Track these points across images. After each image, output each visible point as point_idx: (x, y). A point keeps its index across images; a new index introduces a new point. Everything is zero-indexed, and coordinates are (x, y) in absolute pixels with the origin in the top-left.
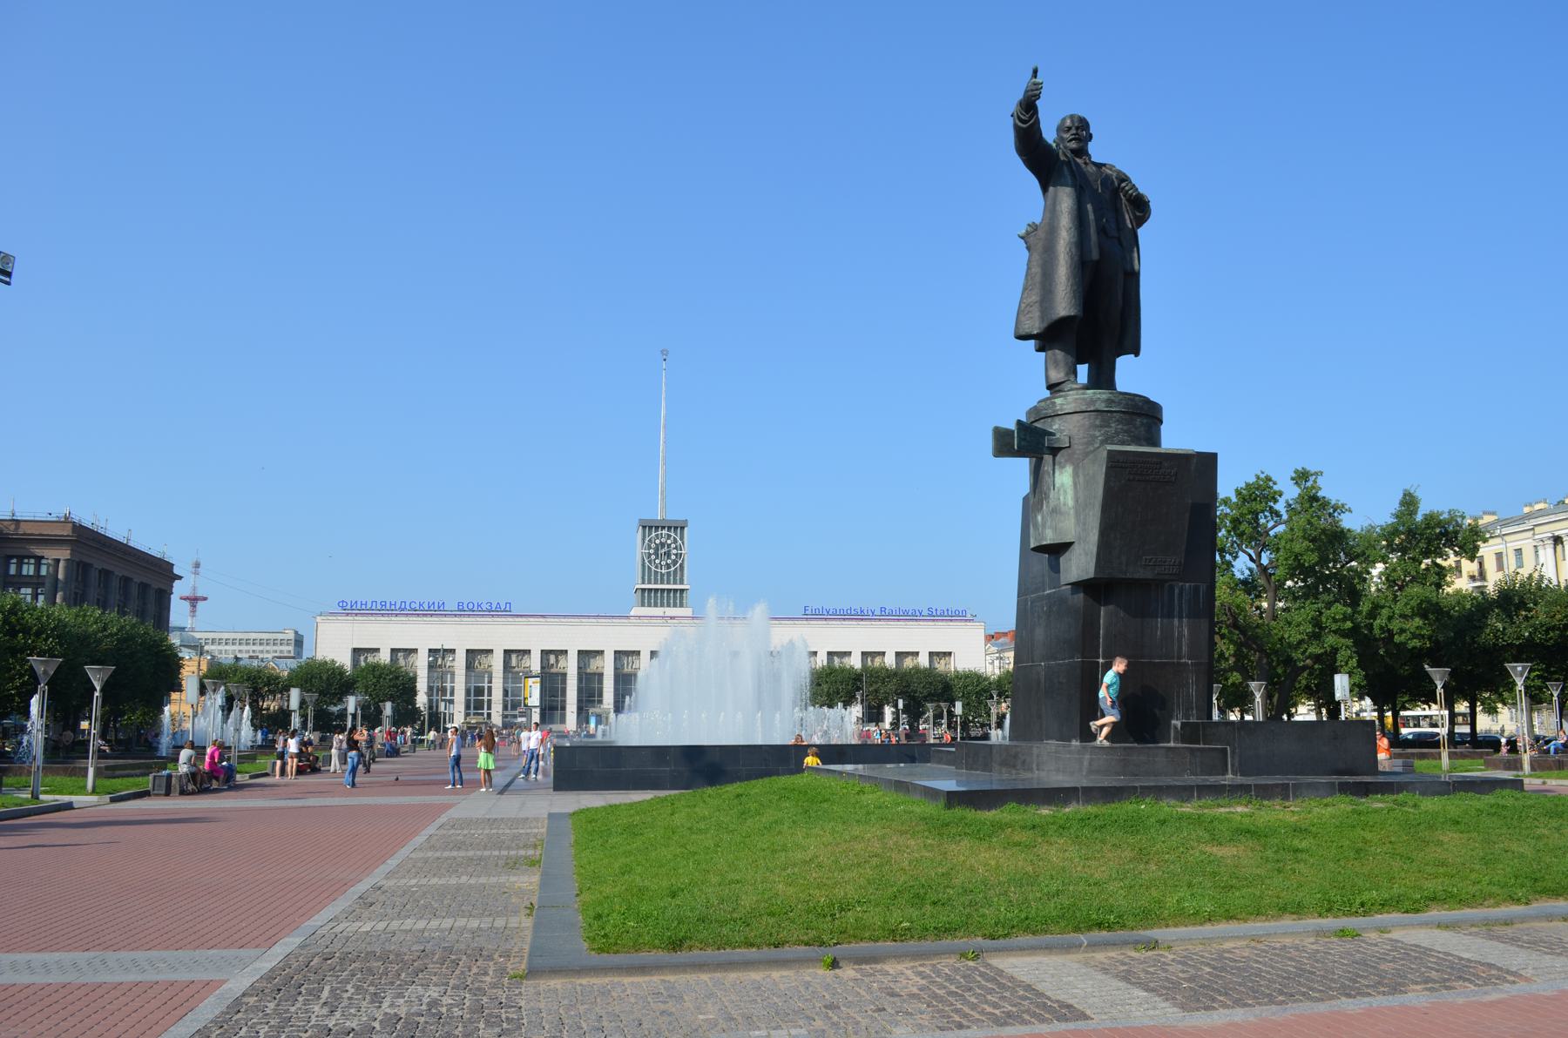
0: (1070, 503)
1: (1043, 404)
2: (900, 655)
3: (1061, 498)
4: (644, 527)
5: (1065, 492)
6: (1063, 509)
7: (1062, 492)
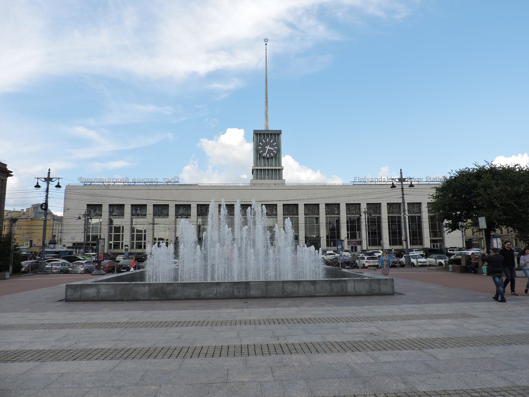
4: (257, 134)
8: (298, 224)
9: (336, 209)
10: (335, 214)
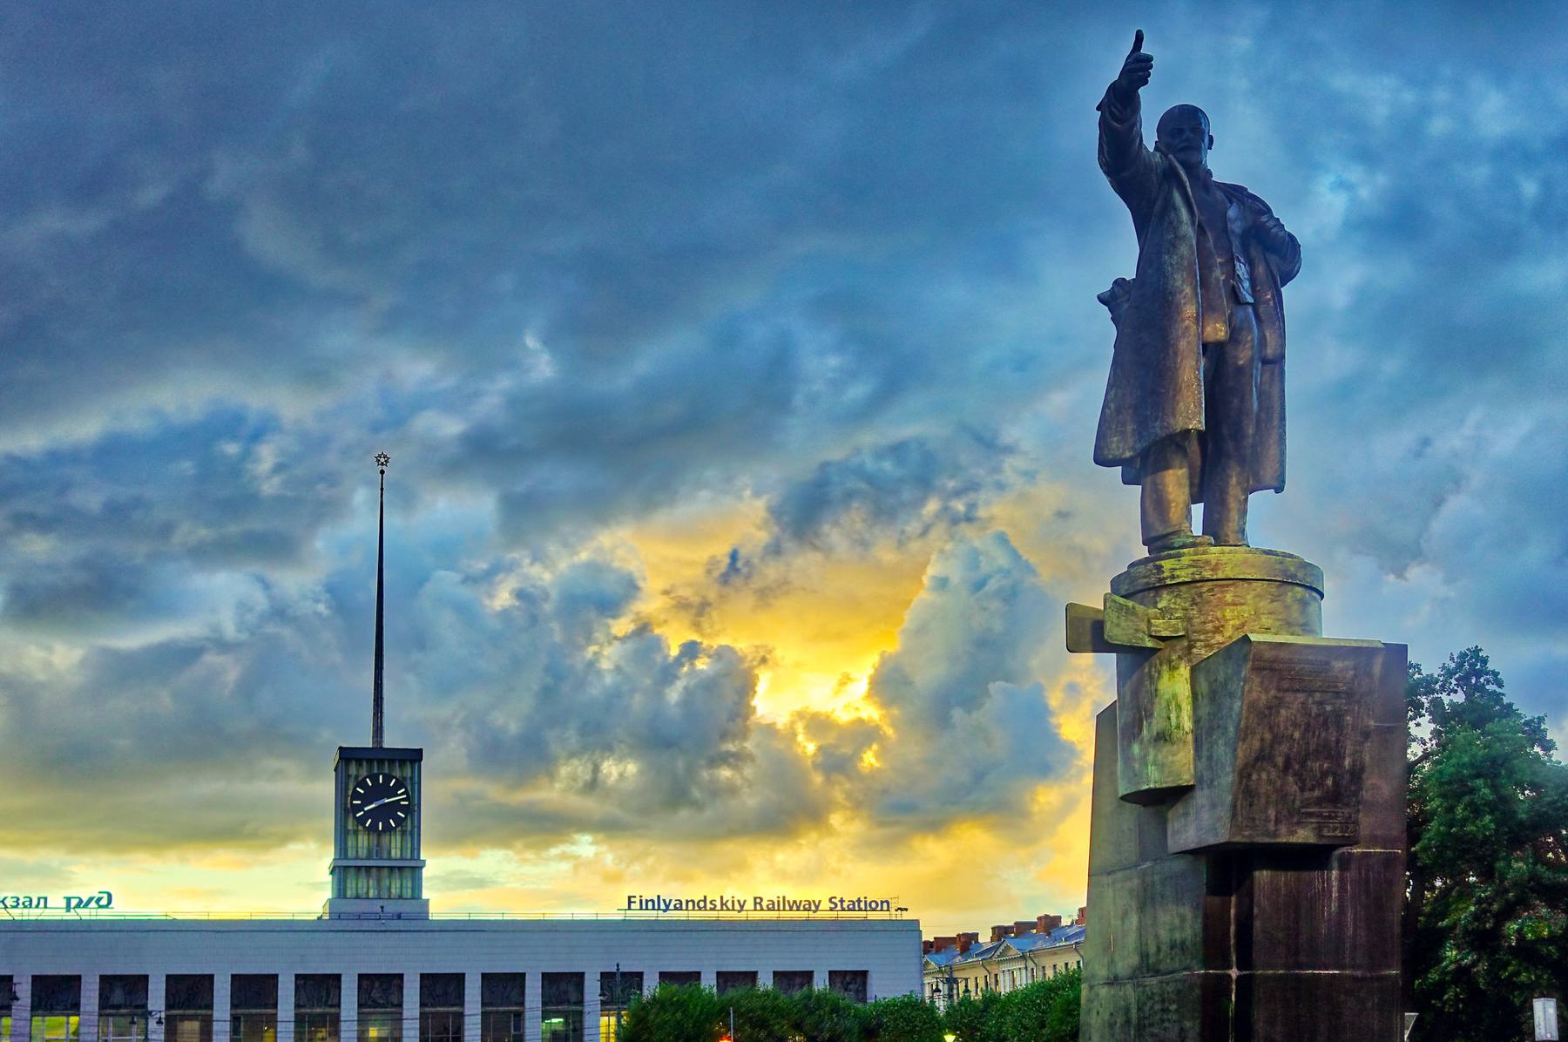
0: (1188, 725)
1: (1141, 569)
2: (724, 978)
3: (1173, 716)
5: (1179, 707)
6: (1177, 734)
7: (1173, 706)
8: (482, 1035)
9: (571, 989)
10: (569, 1002)
